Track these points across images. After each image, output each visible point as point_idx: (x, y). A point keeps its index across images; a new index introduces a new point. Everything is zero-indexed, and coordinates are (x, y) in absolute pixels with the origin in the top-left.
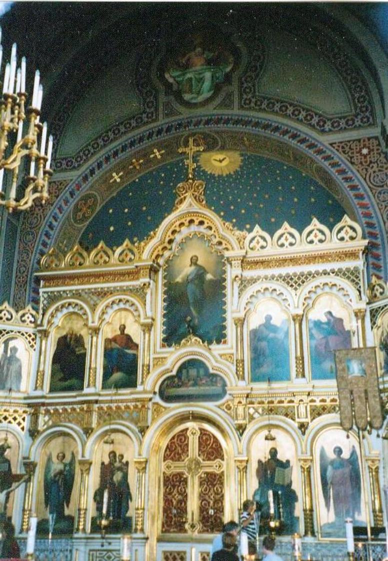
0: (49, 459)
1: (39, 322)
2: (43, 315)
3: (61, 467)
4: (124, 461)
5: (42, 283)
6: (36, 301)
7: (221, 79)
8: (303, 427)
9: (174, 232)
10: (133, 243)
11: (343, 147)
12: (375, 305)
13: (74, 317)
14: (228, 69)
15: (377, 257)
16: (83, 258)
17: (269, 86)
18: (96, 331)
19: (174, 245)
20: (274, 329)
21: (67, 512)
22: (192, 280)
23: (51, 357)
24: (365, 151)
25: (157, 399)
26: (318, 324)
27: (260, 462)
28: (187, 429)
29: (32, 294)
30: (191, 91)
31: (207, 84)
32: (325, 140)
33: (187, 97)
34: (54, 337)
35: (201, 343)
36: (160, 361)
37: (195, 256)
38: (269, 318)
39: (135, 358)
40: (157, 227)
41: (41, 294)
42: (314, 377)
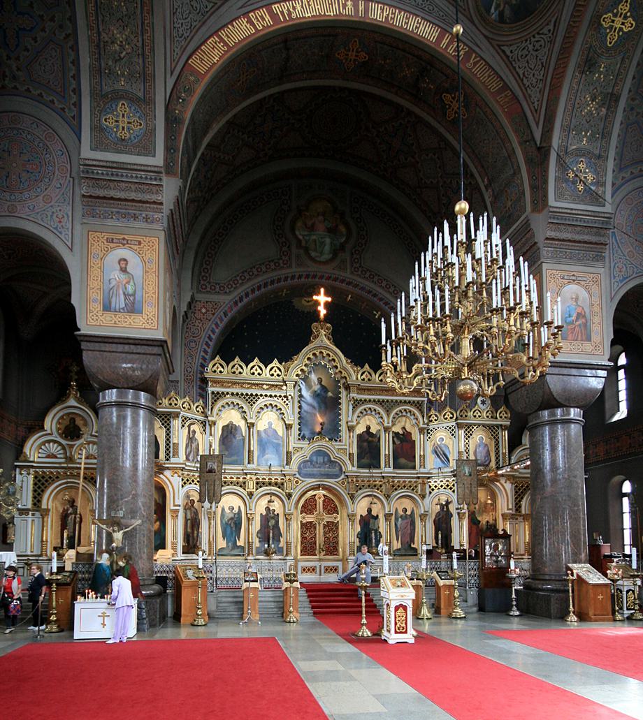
0: (223, 509)
1: (209, 413)
2: (212, 409)
4: (276, 513)
5: (210, 384)
6: (203, 395)
14: (343, 240)
16: (242, 368)
18: (251, 426)
23: (218, 440)
25: (297, 476)
27: (361, 516)
28: (315, 495)
29: (199, 391)
30: (315, 250)
31: (327, 248)
33: (313, 254)
36: (297, 449)
40: (298, 353)
41: (209, 392)
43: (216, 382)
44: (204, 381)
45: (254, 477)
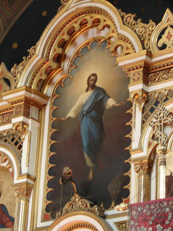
9: (63, 45)
10: (9, 70)
19: (66, 64)
22: (88, 112)
35: (89, 205)
37: (94, 75)
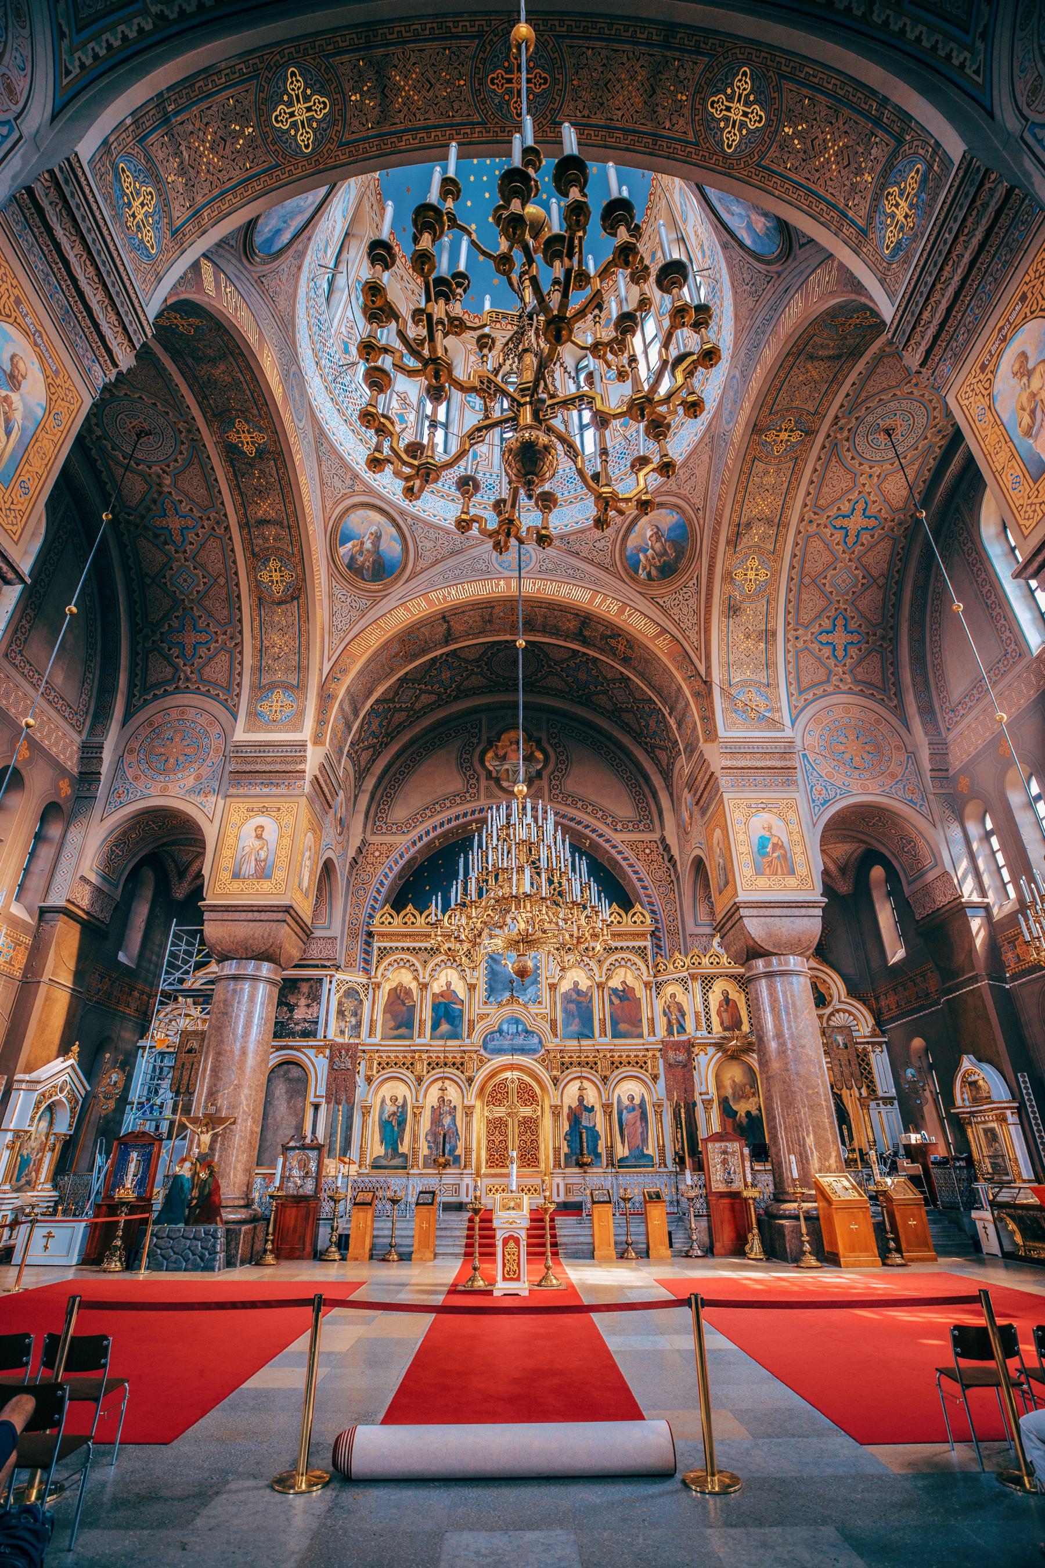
0: (383, 1101)
3: (394, 1109)
7: (534, 774)
8: (605, 1079)
11: (632, 845)
12: (659, 979)
13: (403, 971)
14: (539, 767)
15: (659, 938)
17: (571, 785)
18: (424, 987)
20: (578, 992)
21: (401, 1150)
24: (647, 851)
25: (482, 1052)
26: (615, 991)
30: (508, 780)
32: (617, 838)
33: (505, 784)
34: (387, 987)
36: (482, 1017)
38: (576, 984)
39: (461, 1011)
42: (614, 1037)
43: (382, 935)
44: (370, 934)
45: (424, 1056)
